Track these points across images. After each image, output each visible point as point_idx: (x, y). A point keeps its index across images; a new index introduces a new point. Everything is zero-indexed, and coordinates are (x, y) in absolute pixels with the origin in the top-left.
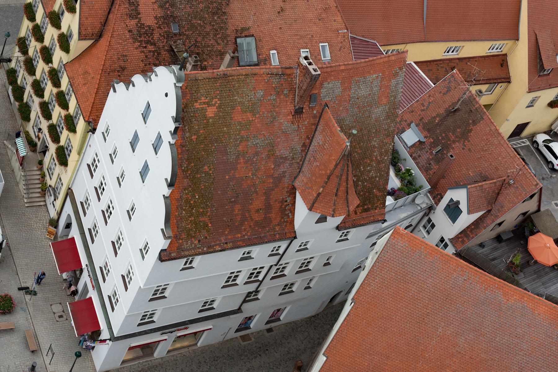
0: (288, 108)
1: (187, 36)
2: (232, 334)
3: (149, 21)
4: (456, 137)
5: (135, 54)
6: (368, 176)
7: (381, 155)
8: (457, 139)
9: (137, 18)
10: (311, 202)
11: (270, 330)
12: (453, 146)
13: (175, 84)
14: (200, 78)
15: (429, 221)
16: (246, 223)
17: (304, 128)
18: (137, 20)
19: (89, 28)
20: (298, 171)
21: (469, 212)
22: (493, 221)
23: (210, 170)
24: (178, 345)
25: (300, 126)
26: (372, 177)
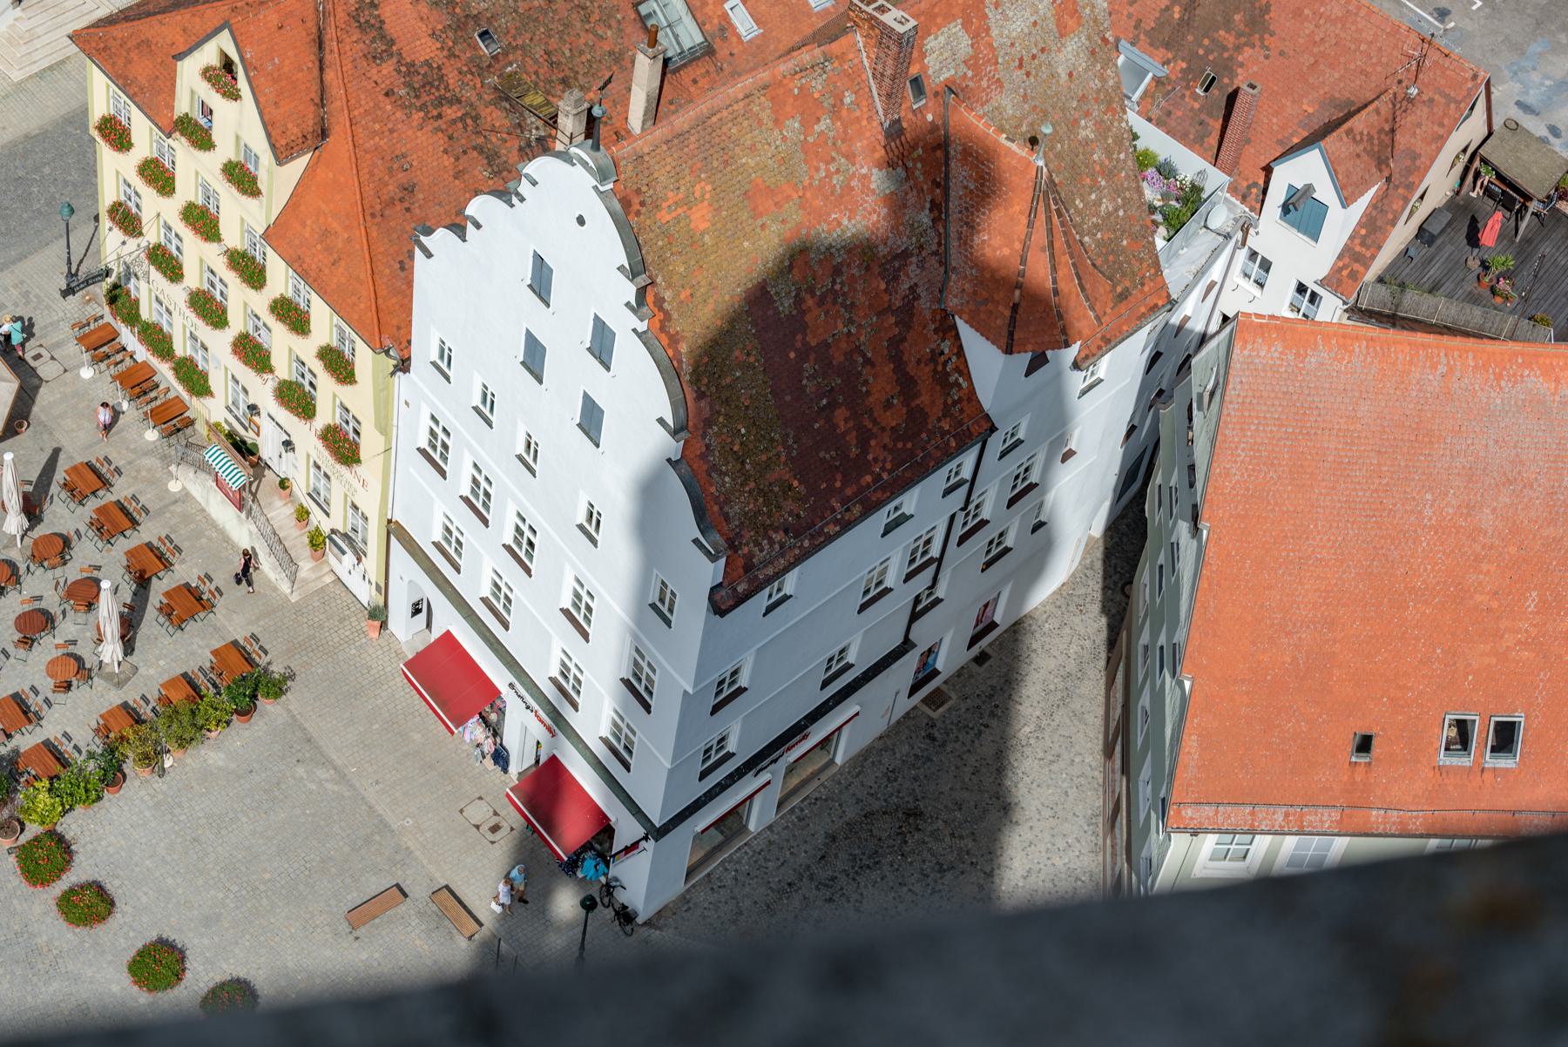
0: (868, 134)
1: (523, 48)
2: (905, 704)
3: (424, 49)
4: (1240, 35)
5: (424, 146)
6: (1097, 215)
7: (1109, 152)
8: (1243, 40)
9: (392, 55)
10: (1005, 333)
11: (981, 659)
12: (1240, 58)
13: (595, 188)
14: (646, 150)
15: (1253, 255)
16: (873, 443)
17: (919, 165)
18: (395, 60)
19: (290, 126)
20: (942, 270)
21: (1346, 202)
22: (1406, 200)
23: (748, 354)
24: (795, 781)
25: (910, 164)
26: (1109, 214)
